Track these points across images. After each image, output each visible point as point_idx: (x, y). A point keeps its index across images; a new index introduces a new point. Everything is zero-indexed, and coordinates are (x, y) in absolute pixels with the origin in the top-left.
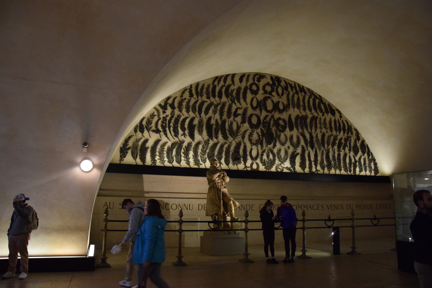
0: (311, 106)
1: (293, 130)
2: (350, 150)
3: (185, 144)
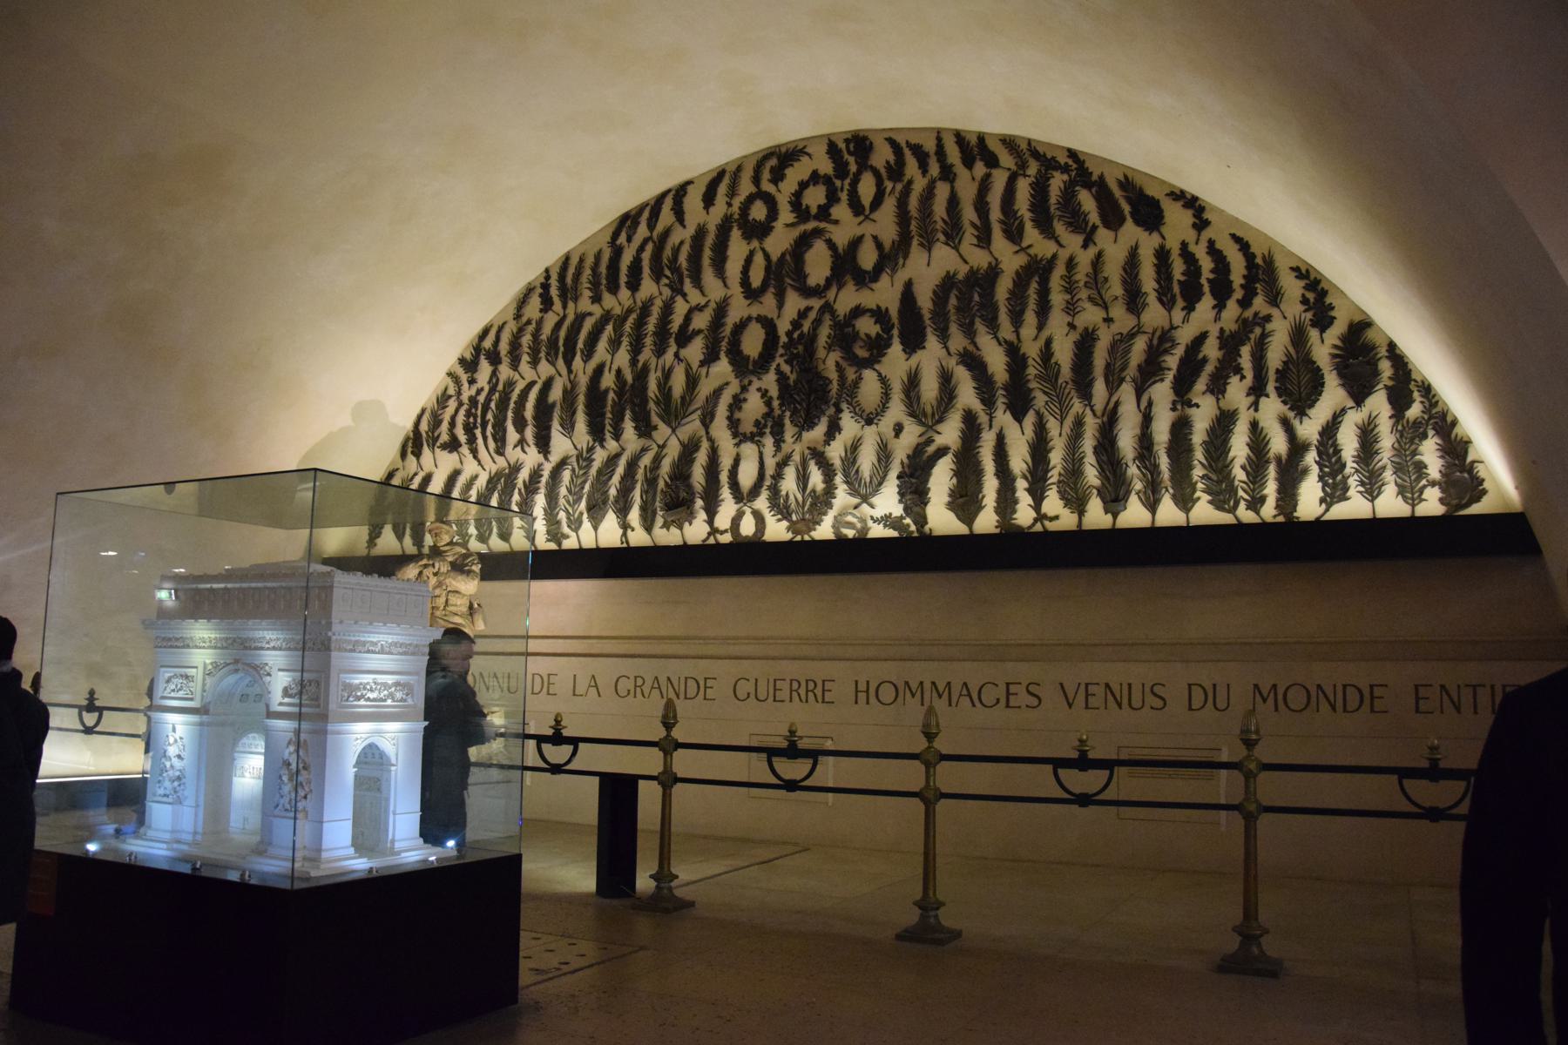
0: (1019, 214)
1: (924, 347)
2: (1257, 391)
3: (524, 475)
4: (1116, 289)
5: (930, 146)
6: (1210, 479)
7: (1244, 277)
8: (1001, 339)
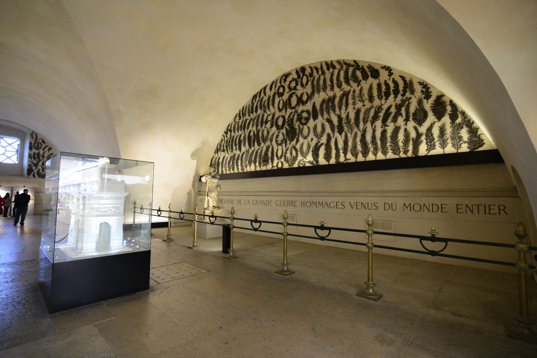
0: (341, 80)
2: (407, 120)
3: (236, 156)
4: (366, 96)
5: (319, 67)
6: (392, 146)
7: (403, 87)
8: (336, 114)
